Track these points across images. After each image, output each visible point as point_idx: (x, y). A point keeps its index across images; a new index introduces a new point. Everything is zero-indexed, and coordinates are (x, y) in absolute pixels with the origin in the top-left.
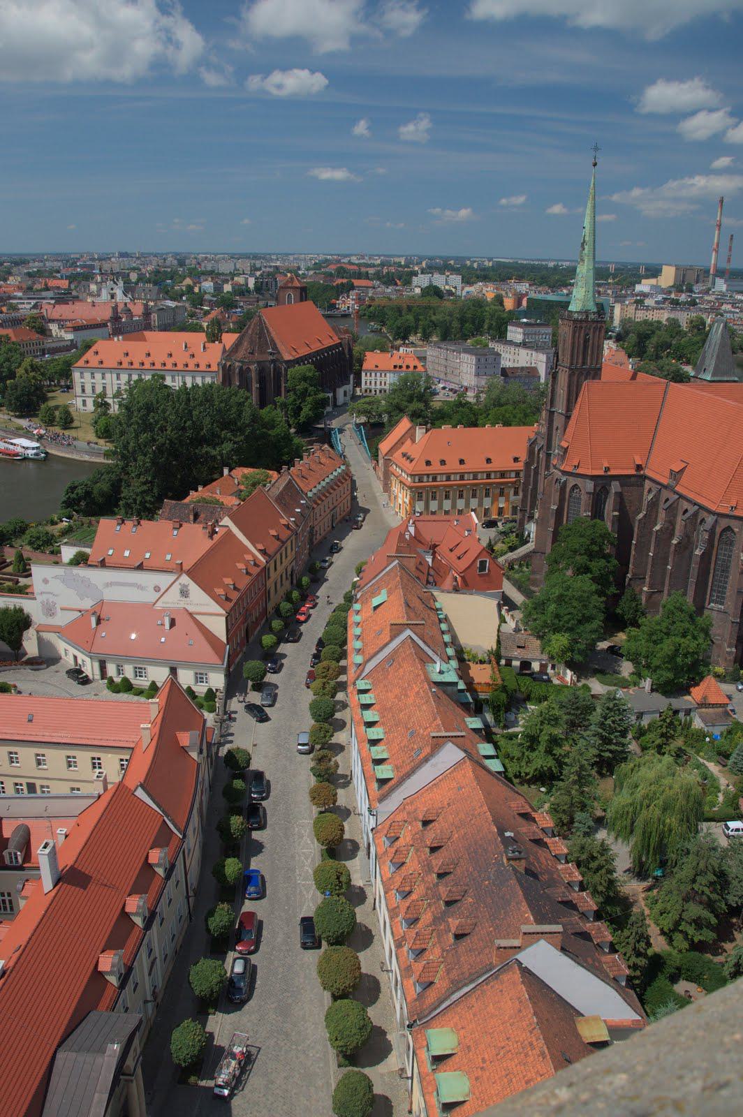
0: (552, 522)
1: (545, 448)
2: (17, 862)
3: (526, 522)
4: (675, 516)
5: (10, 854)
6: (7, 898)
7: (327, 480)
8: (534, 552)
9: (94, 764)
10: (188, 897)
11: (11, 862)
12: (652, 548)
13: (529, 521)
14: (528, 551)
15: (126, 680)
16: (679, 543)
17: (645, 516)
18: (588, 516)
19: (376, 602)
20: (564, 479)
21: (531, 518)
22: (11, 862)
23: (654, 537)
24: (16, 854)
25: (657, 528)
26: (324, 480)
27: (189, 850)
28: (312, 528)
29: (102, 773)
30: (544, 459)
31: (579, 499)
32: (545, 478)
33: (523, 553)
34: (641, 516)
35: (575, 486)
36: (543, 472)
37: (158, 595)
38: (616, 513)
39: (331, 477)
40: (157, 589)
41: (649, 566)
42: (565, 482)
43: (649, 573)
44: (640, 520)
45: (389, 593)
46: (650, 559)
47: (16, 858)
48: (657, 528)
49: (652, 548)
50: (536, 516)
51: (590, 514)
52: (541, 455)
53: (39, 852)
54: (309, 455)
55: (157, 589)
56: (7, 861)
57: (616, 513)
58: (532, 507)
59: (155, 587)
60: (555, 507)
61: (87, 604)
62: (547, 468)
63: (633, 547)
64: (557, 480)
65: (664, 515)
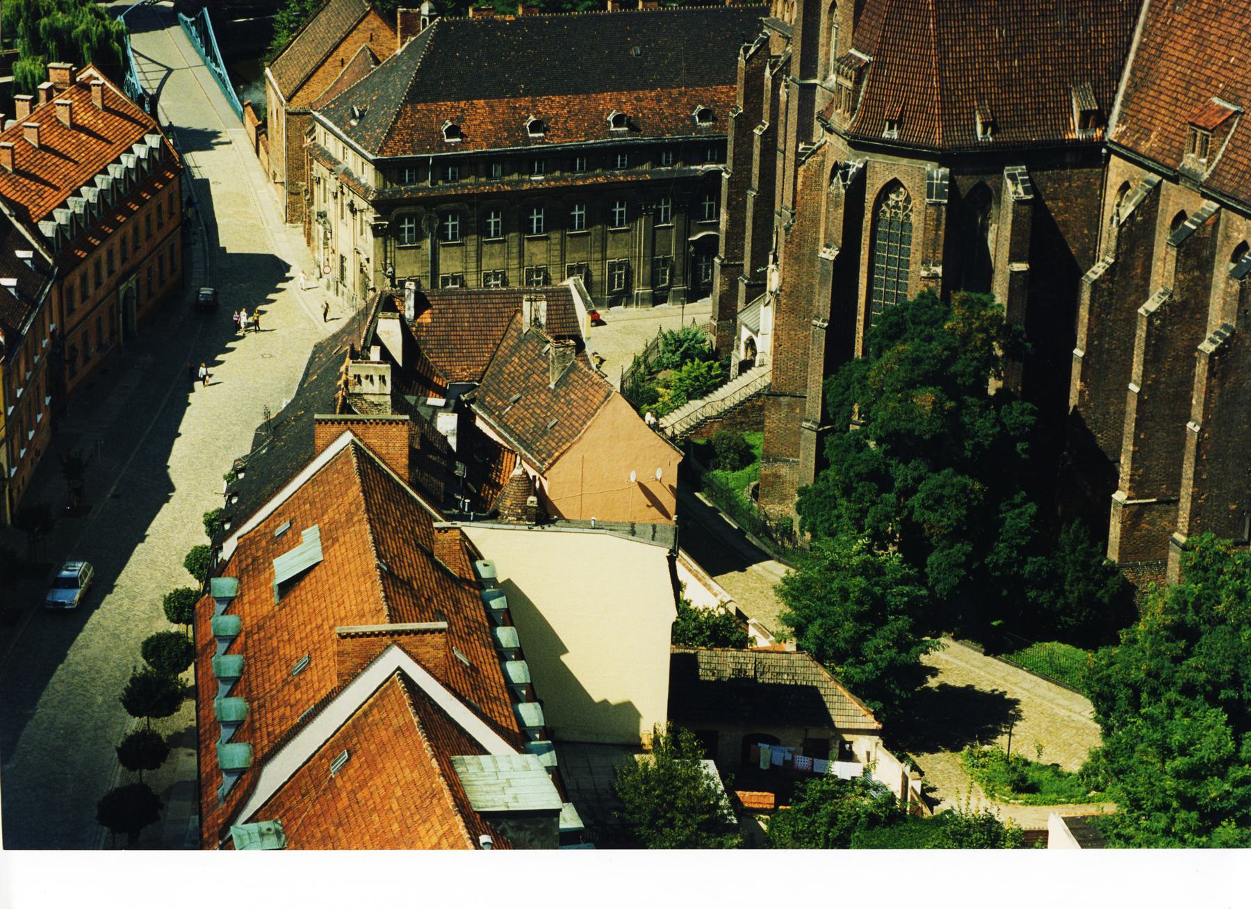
0: (823, 300)
1: (795, 69)
3: (741, 305)
4: (1206, 266)
7: (102, 182)
8: (770, 394)
12: (1137, 369)
13: (749, 299)
14: (751, 391)
16: (1219, 351)
17: (1111, 270)
18: (934, 277)
19: (285, 566)
20: (856, 164)
21: (757, 288)
23: (1141, 332)
25: (1152, 305)
26: (91, 183)
28: (58, 339)
30: (794, 104)
31: (905, 225)
32: (798, 164)
33: (737, 399)
34: (1098, 270)
35: (894, 185)
36: (788, 141)
38: (1021, 267)
39: (115, 172)
41: (1130, 427)
42: (862, 174)
43: (1128, 446)
44: (1095, 284)
45: (328, 539)
46: (1132, 405)
48: (1152, 305)
49: (1137, 369)
50: (774, 280)
51: (939, 270)
52: (783, 93)
54: (34, 102)
57: (1021, 267)
58: (760, 259)
60: (829, 254)
62: (805, 133)
63: (1076, 369)
64: (836, 167)
65: (1171, 265)
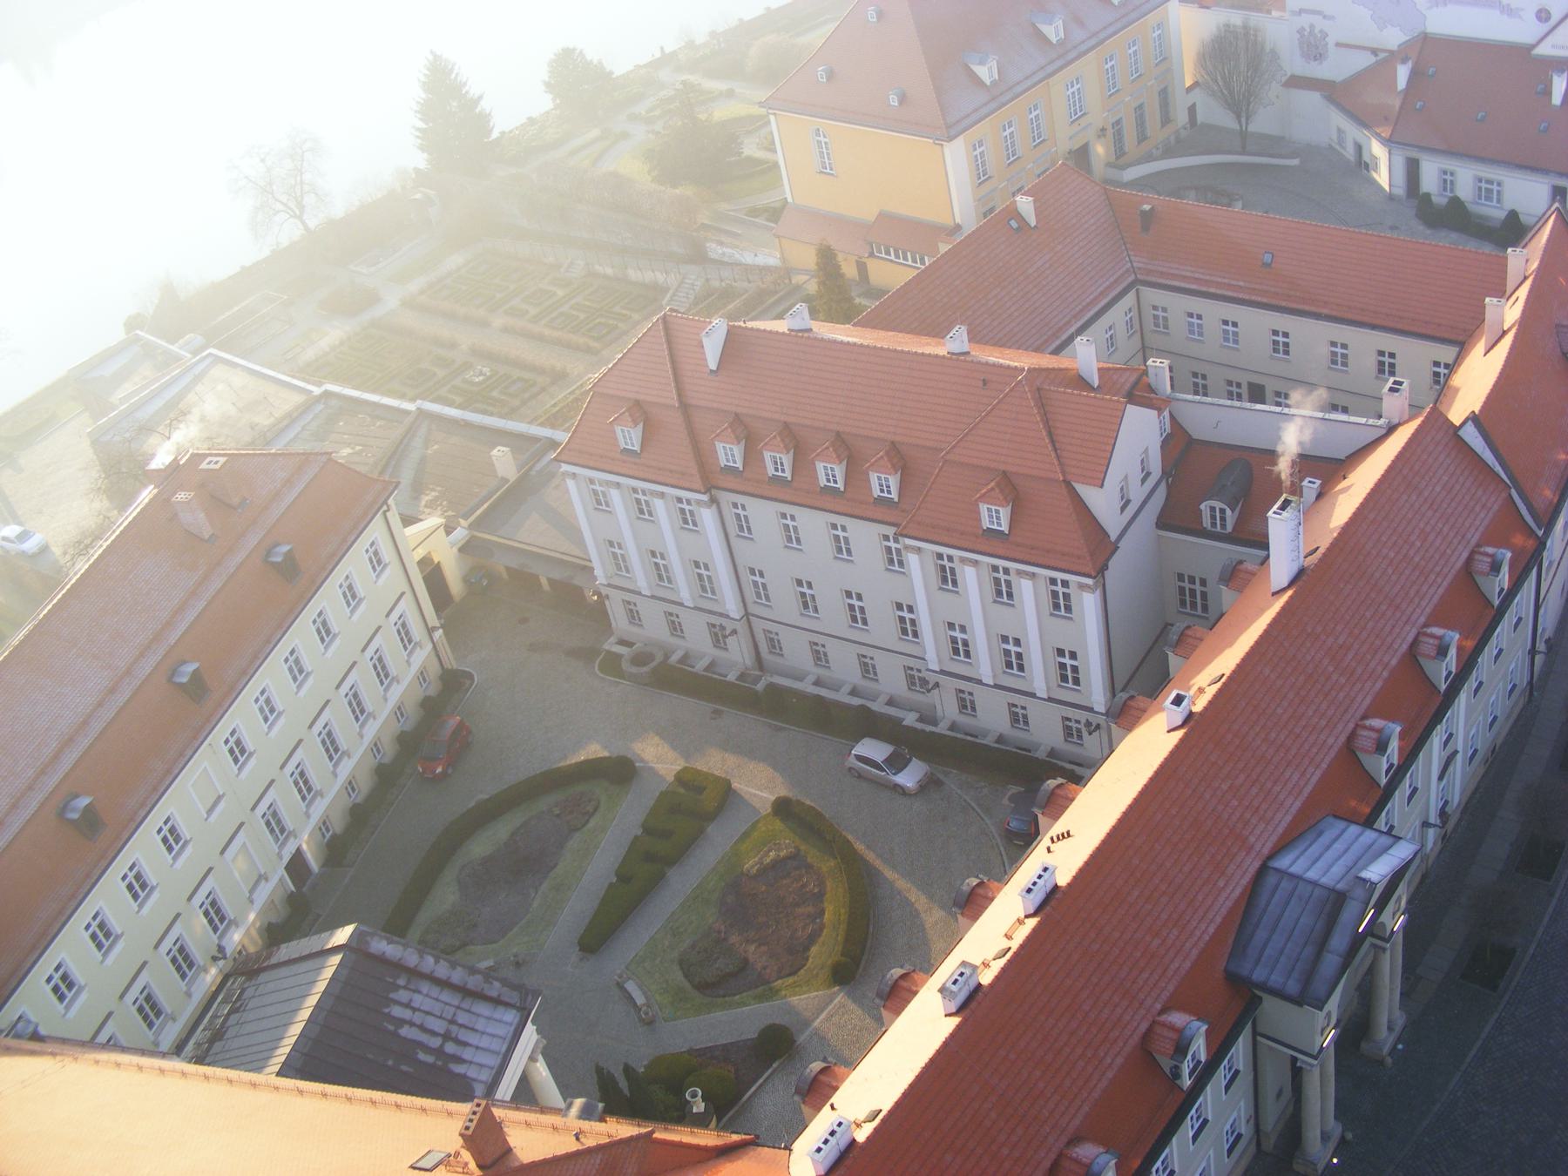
2: (1223, 526)
5: (1213, 509)
6: (1198, 587)
9: (1381, 364)
10: (1533, 652)
11: (1214, 524)
15: (1456, 203)
22: (1214, 524)
24: (1222, 511)
27: (1551, 563)
29: (1400, 383)
37: (1545, 27)
40: (1543, 15)
47: (1223, 519)
53: (1270, 513)
55: (1543, 15)
56: (1207, 522)
59: (1540, 11)
61: (1393, 38)
